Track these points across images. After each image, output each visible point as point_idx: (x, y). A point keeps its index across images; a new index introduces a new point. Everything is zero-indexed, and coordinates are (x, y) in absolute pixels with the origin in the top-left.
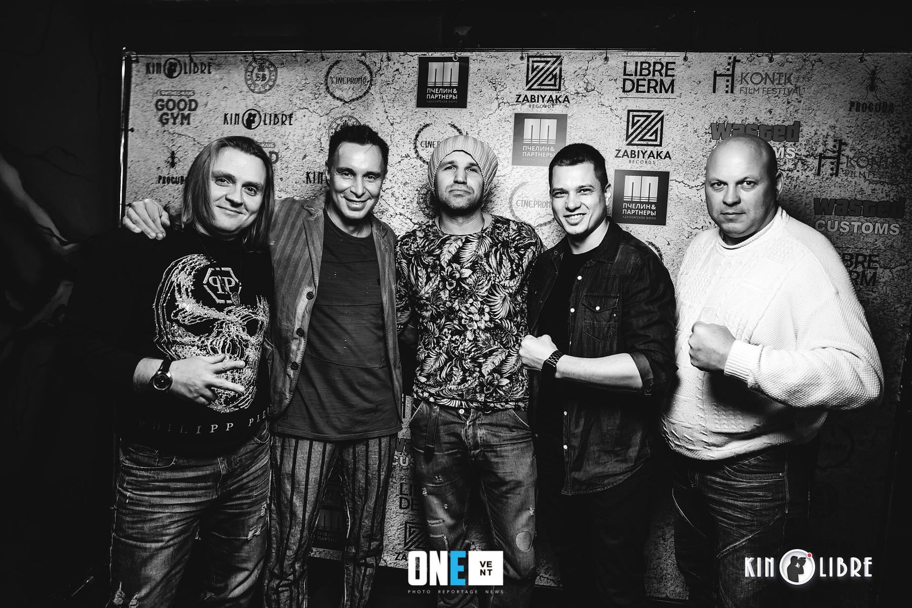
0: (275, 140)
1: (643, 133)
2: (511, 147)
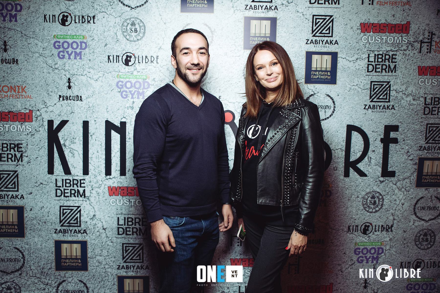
0: (84, 33)
1: (322, 29)
2: (243, 38)
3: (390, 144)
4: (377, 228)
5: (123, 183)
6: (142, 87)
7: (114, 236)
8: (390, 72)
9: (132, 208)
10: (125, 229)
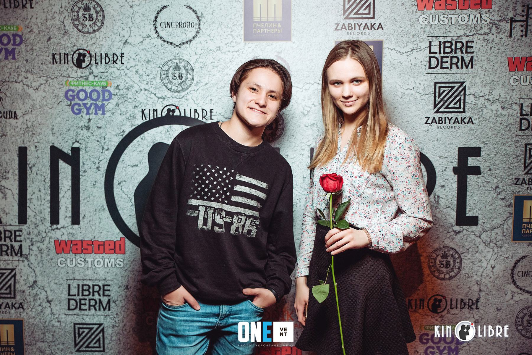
3: (468, 176)
4: (454, 303)
5: (76, 236)
6: (101, 98)
7: (62, 311)
8: (464, 67)
9: (89, 271)
10: (78, 301)
